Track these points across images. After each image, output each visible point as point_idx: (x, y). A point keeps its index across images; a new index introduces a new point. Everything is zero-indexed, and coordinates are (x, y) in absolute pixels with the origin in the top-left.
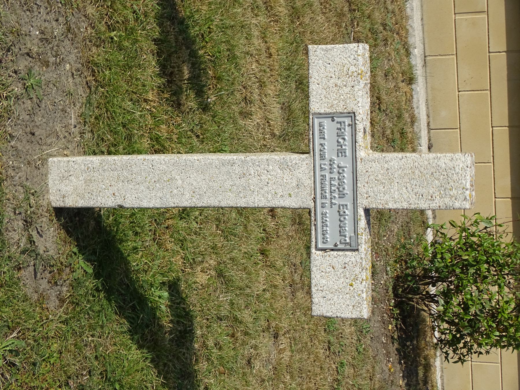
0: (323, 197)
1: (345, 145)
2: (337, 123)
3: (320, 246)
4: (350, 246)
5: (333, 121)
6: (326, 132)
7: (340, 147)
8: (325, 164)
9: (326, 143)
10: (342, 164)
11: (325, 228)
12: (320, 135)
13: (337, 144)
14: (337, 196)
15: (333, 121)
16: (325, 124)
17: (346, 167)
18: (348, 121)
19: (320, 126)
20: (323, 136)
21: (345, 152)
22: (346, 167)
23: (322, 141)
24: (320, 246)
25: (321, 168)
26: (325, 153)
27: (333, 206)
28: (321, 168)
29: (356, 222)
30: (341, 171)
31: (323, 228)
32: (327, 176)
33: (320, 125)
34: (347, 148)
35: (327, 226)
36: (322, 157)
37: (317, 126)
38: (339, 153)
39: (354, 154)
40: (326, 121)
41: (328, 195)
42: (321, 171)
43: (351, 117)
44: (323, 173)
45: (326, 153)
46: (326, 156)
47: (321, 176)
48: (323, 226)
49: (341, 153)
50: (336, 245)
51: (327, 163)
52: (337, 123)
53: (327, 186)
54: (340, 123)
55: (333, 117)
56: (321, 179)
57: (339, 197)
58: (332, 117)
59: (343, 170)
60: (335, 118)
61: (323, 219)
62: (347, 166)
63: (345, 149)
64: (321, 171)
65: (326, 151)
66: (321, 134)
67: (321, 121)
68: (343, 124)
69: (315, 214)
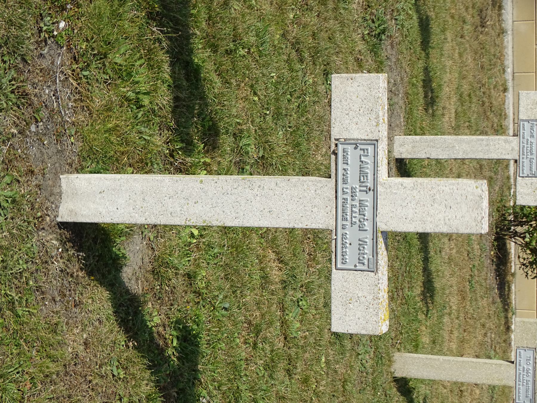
2: (361, 149)
4: (368, 268)
6: (349, 158)
8: (347, 188)
9: (349, 168)
11: (344, 250)
12: (343, 161)
16: (349, 150)
18: (370, 148)
19: (344, 152)
20: (347, 162)
23: (345, 166)
24: (339, 266)
25: (343, 192)
28: (343, 192)
31: (342, 250)
32: (349, 199)
35: (346, 248)
37: (341, 153)
40: (349, 148)
42: (343, 194)
43: (374, 145)
45: (349, 178)
46: (349, 181)
47: (343, 199)
48: (342, 247)
50: (355, 266)
51: (349, 187)
52: (361, 149)
53: (348, 209)
54: (364, 150)
56: (343, 202)
61: (343, 241)
64: (343, 194)
65: (349, 176)
67: (345, 147)
68: (366, 151)
69: (336, 164)
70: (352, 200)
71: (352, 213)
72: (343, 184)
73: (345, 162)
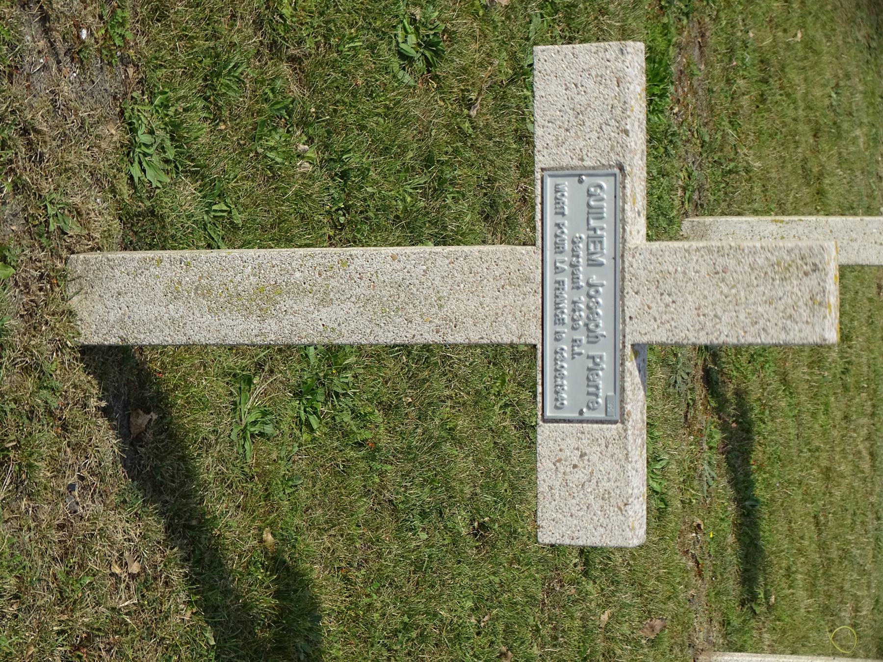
1: (602, 229)
7: (592, 233)
10: (594, 279)
13: (587, 209)
14: (584, 339)
17: (602, 285)
21: (601, 242)
22: (602, 285)
27: (576, 356)
29: (619, 362)
30: (592, 293)
34: (605, 234)
38: (590, 242)
39: (619, 283)
49: (594, 242)
57: (588, 342)
59: (597, 292)
62: (605, 282)
63: (602, 237)
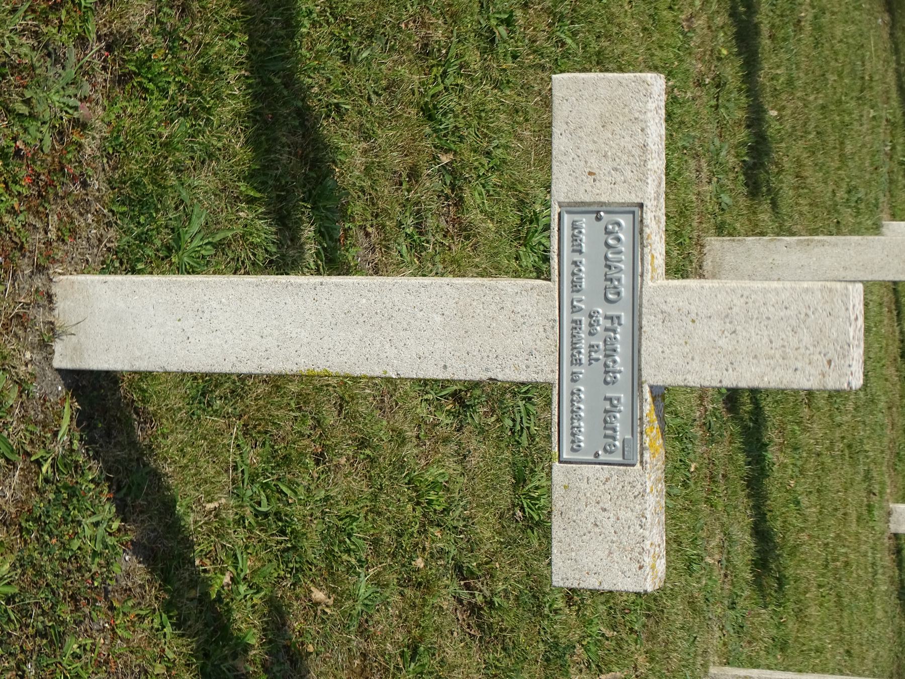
0: (575, 361)
3: (565, 456)
5: (598, 219)
6: (584, 238)
8: (580, 301)
9: (584, 260)
11: (576, 424)
12: (573, 245)
15: (598, 219)
16: (584, 225)
19: (574, 228)
20: (579, 248)
23: (577, 257)
24: (565, 456)
25: (573, 307)
26: (581, 278)
28: (573, 307)
31: (572, 423)
32: (583, 322)
33: (574, 226)
35: (579, 420)
36: (576, 287)
41: (584, 358)
42: (573, 312)
43: (633, 213)
44: (576, 317)
48: (572, 419)
50: (597, 455)
55: (598, 212)
58: (596, 210)
60: (602, 214)
61: (573, 405)
64: (573, 312)
66: (575, 243)
70: (590, 334)
71: (590, 352)
72: (573, 291)
73: (575, 248)
